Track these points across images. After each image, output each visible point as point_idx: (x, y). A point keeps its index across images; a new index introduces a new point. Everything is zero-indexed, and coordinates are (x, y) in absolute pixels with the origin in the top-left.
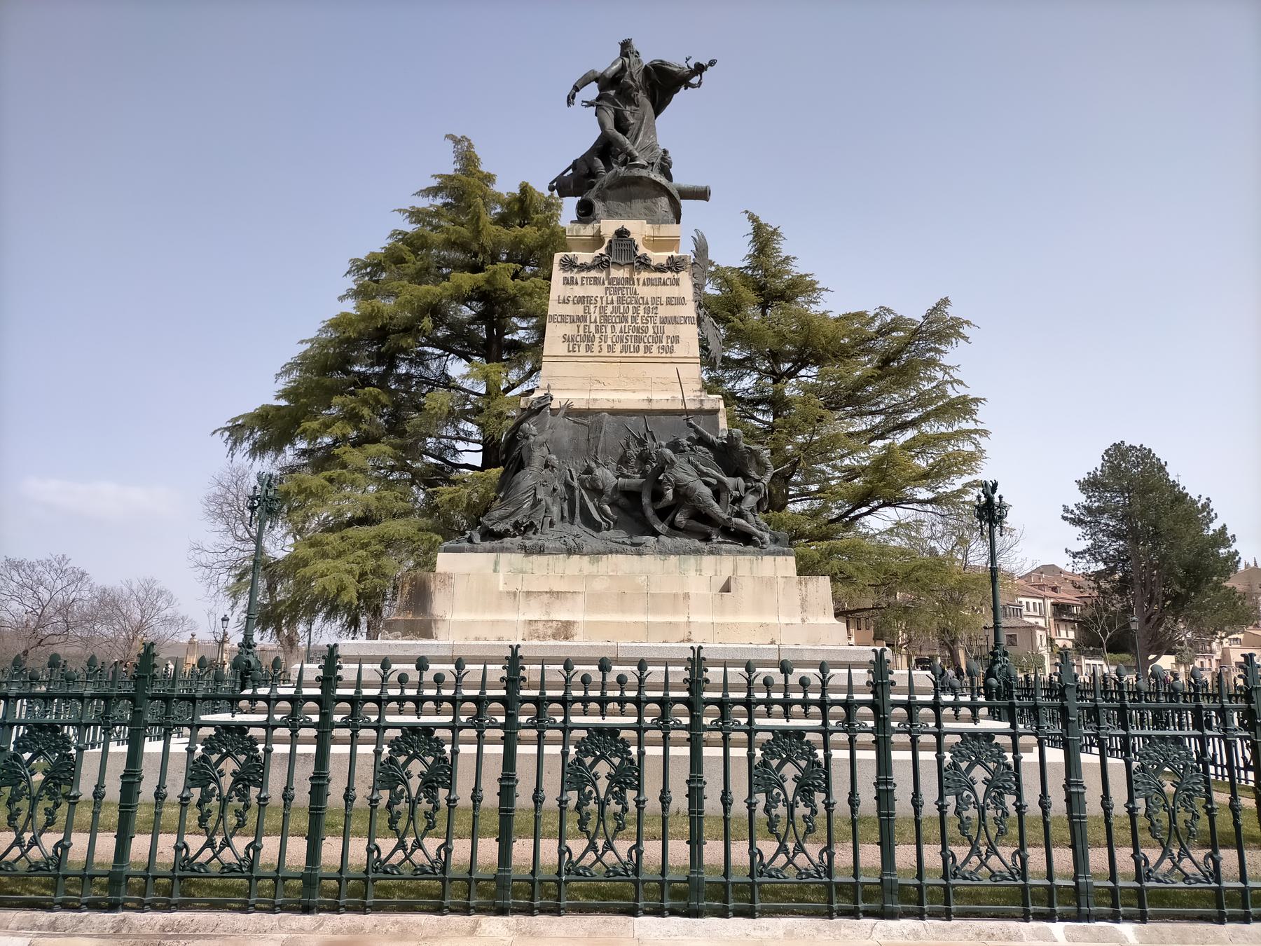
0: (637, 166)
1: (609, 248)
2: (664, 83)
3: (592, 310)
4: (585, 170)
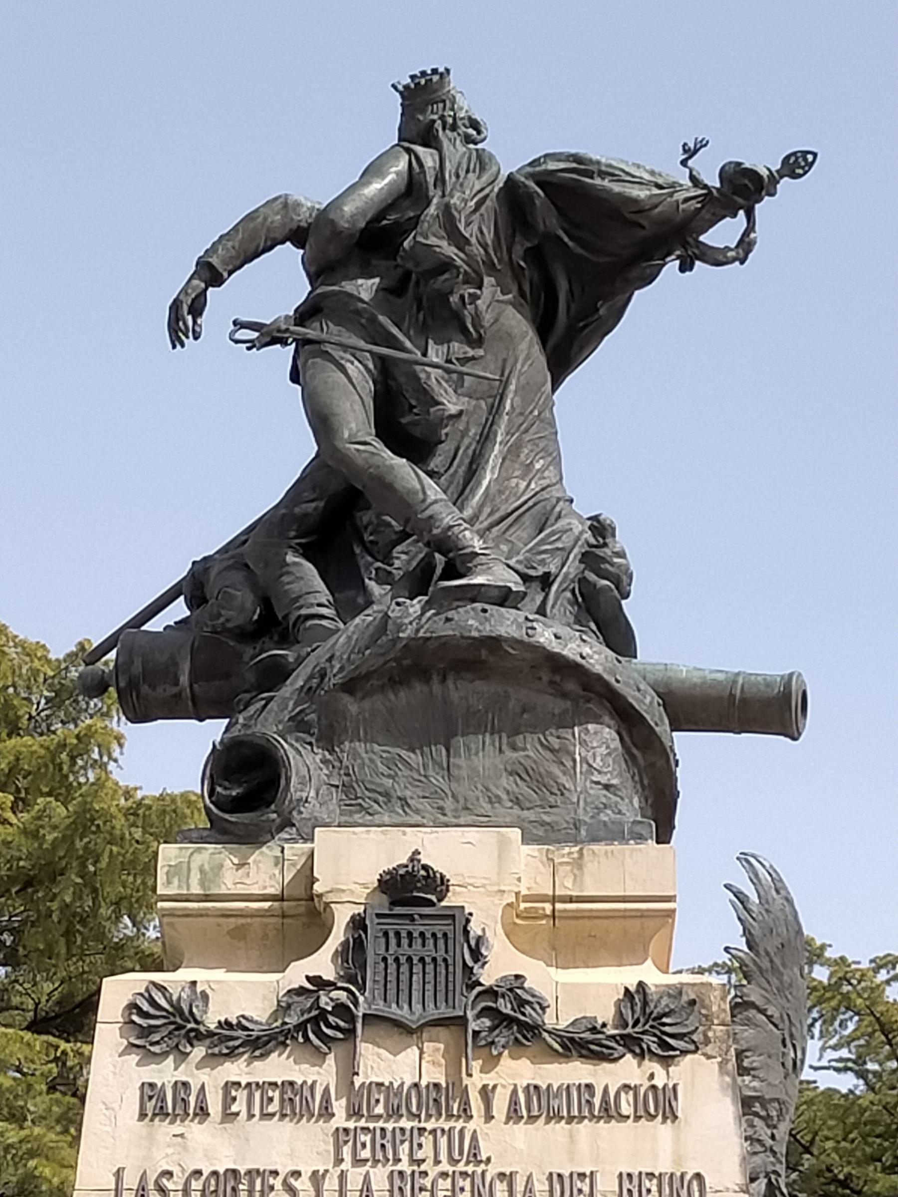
0: (474, 594)
1: (353, 953)
2: (586, 249)
4: (243, 605)
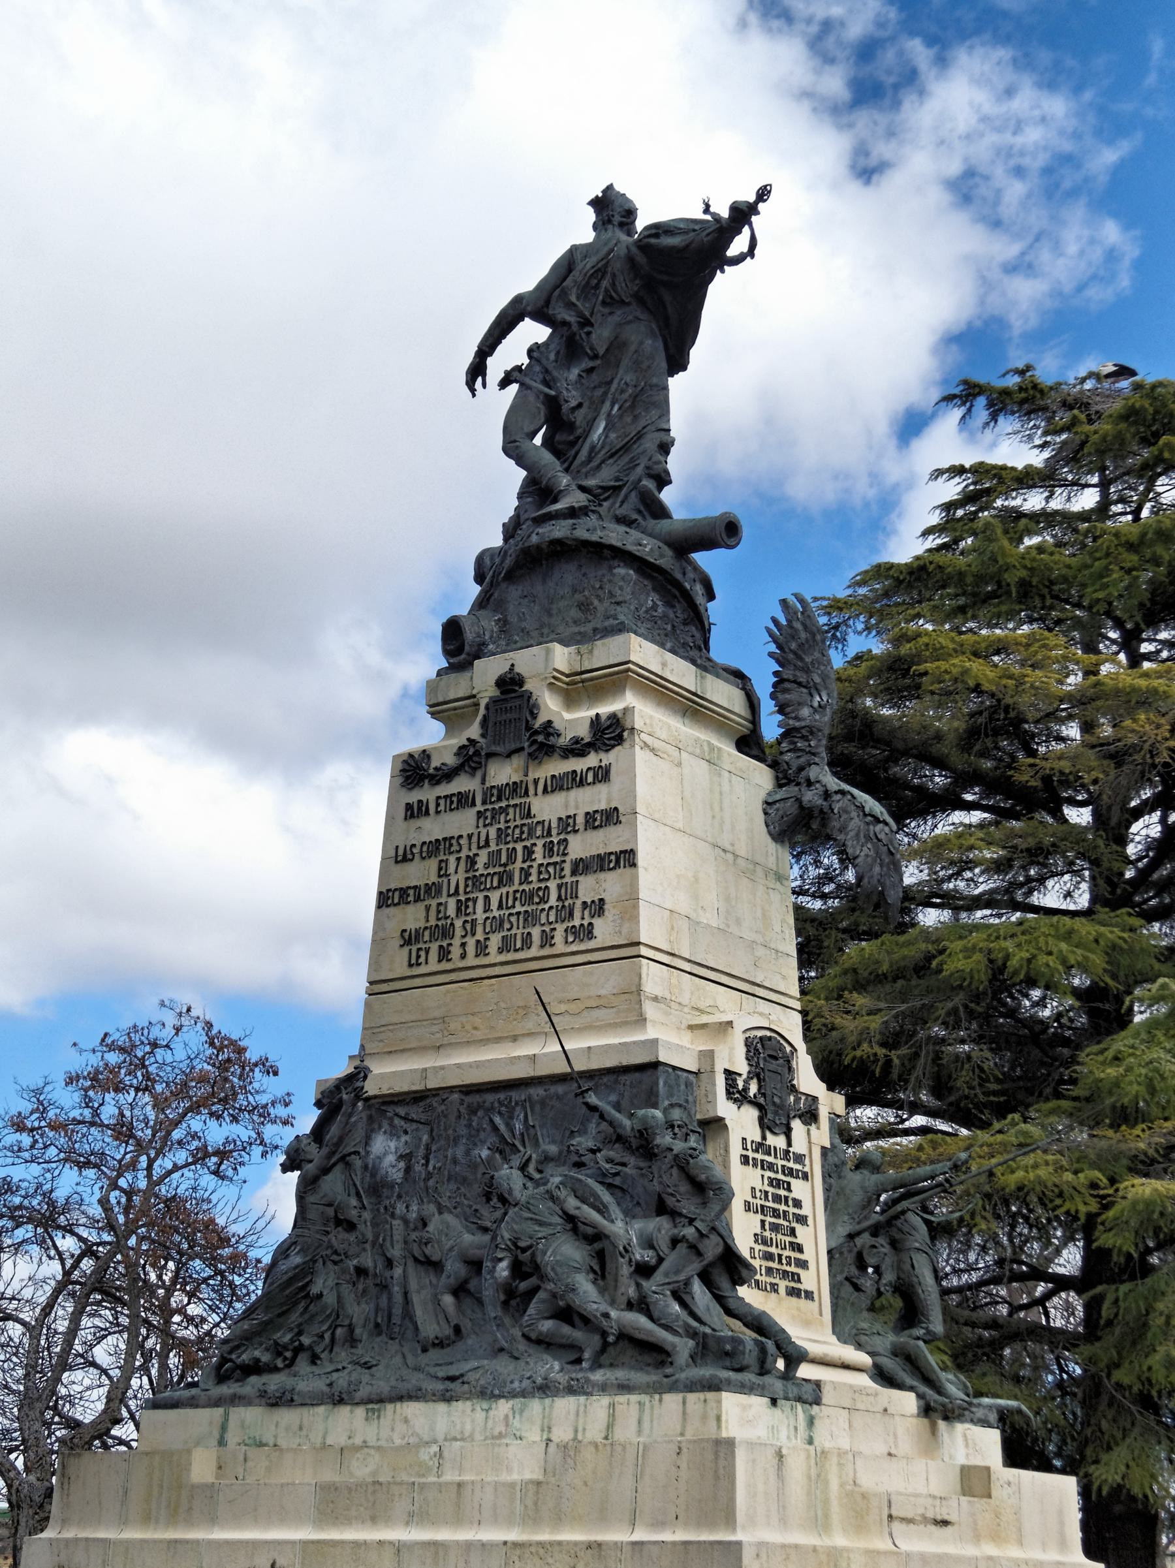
3: (451, 870)
